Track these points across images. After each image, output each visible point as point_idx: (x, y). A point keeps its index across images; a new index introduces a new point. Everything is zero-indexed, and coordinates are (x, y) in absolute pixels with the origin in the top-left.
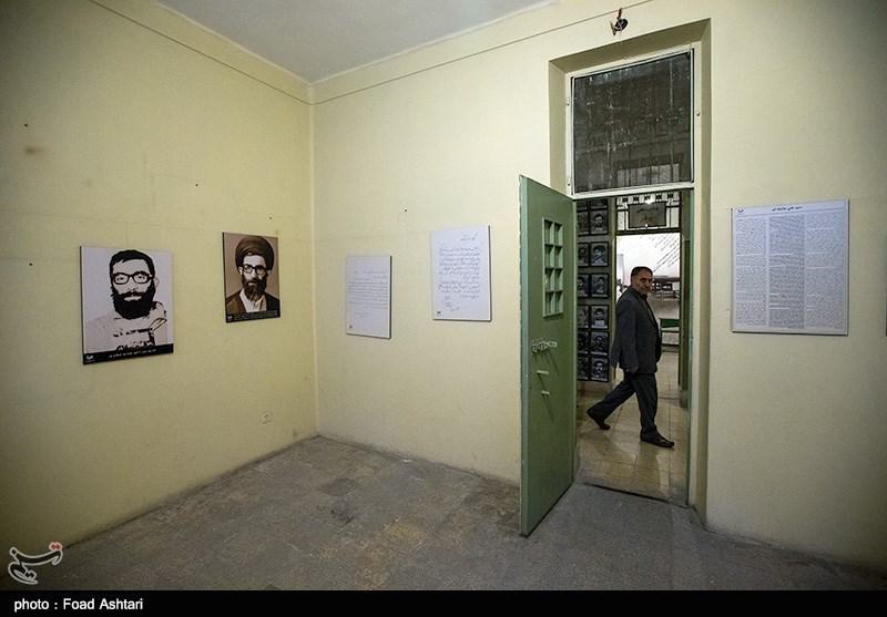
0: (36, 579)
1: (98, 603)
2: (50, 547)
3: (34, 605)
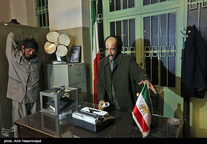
0: (8, 135)
2: (12, 128)
3: (9, 141)
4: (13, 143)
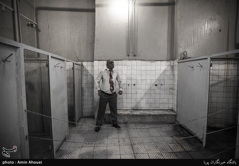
2: (13, 147)
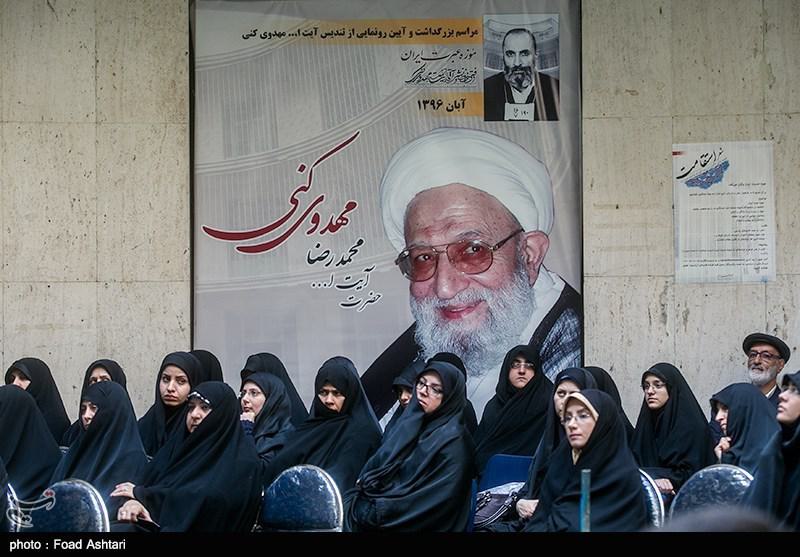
1: (85, 544)
3: (27, 545)
4: (42, 552)
